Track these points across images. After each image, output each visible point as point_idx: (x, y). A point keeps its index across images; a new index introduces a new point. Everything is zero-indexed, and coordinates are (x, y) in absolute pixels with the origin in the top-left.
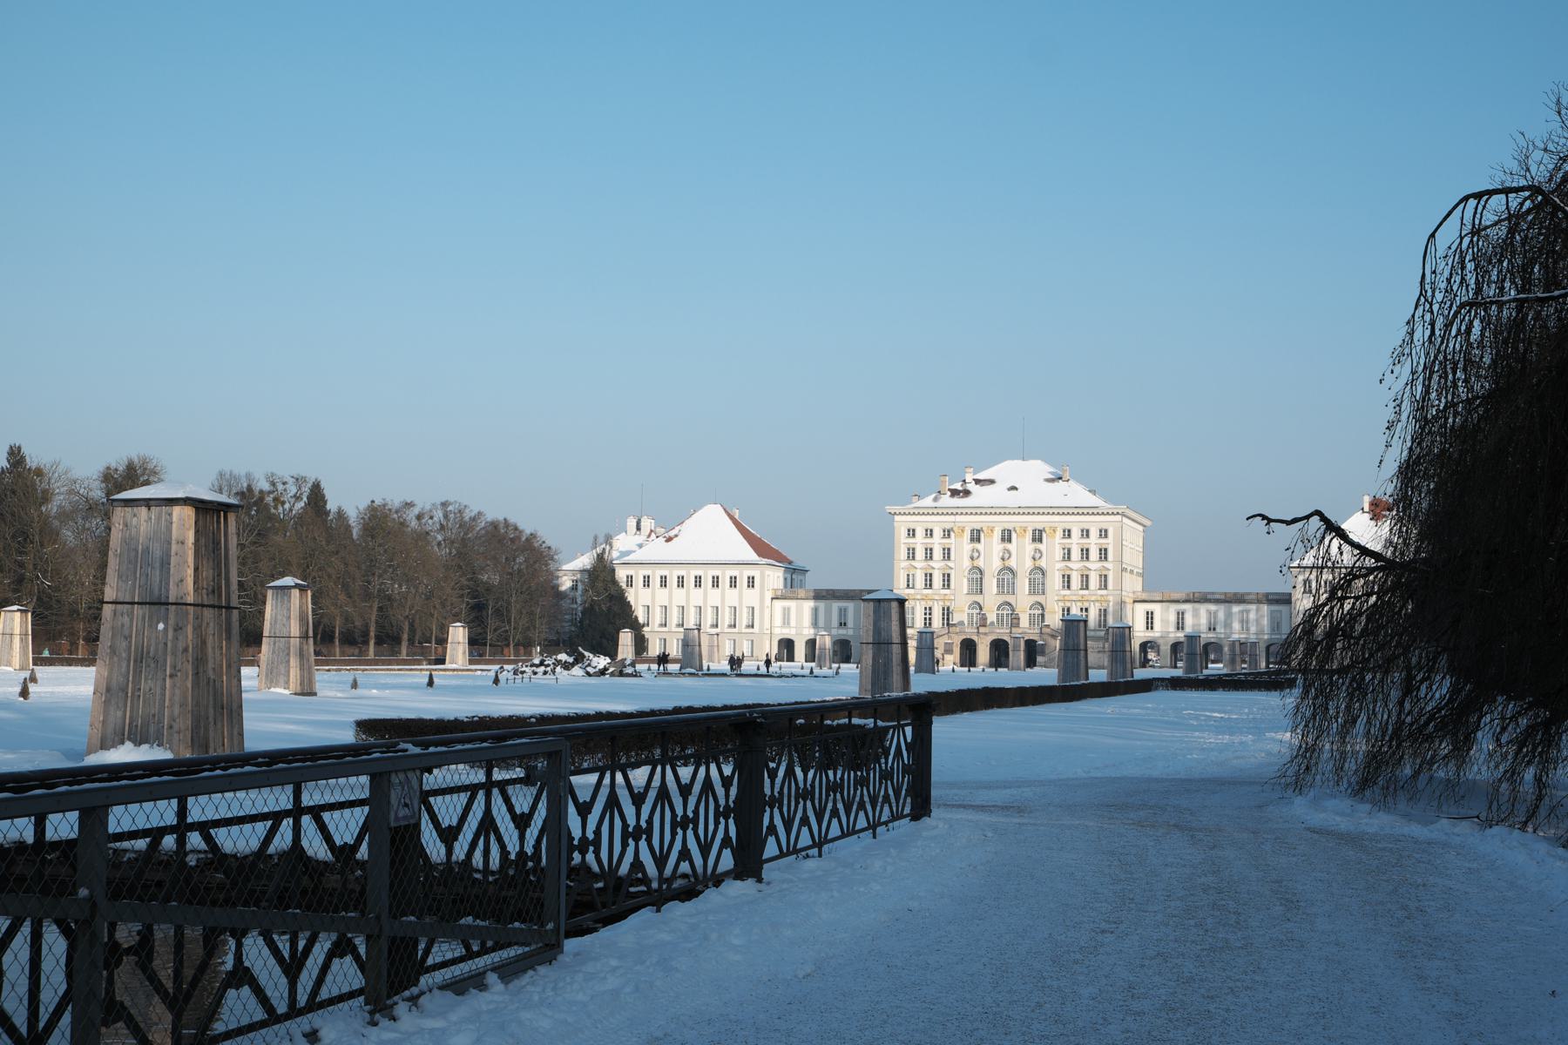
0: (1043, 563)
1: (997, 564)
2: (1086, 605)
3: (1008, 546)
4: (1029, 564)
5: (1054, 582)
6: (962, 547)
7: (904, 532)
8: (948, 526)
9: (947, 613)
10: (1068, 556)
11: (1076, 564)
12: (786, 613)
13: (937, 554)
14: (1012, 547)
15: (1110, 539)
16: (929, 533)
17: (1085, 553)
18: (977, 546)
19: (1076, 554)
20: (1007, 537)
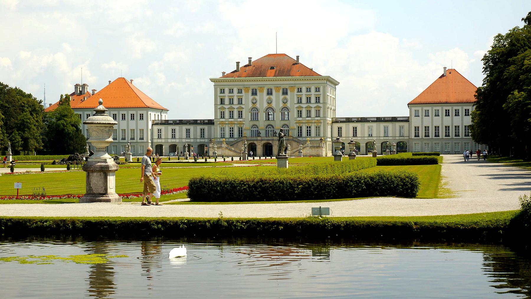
0: (288, 105)
1: (266, 105)
3: (271, 96)
4: (281, 105)
6: (247, 98)
7: (219, 91)
10: (300, 101)
12: (159, 131)
13: (236, 101)
14: (273, 97)
19: (304, 100)
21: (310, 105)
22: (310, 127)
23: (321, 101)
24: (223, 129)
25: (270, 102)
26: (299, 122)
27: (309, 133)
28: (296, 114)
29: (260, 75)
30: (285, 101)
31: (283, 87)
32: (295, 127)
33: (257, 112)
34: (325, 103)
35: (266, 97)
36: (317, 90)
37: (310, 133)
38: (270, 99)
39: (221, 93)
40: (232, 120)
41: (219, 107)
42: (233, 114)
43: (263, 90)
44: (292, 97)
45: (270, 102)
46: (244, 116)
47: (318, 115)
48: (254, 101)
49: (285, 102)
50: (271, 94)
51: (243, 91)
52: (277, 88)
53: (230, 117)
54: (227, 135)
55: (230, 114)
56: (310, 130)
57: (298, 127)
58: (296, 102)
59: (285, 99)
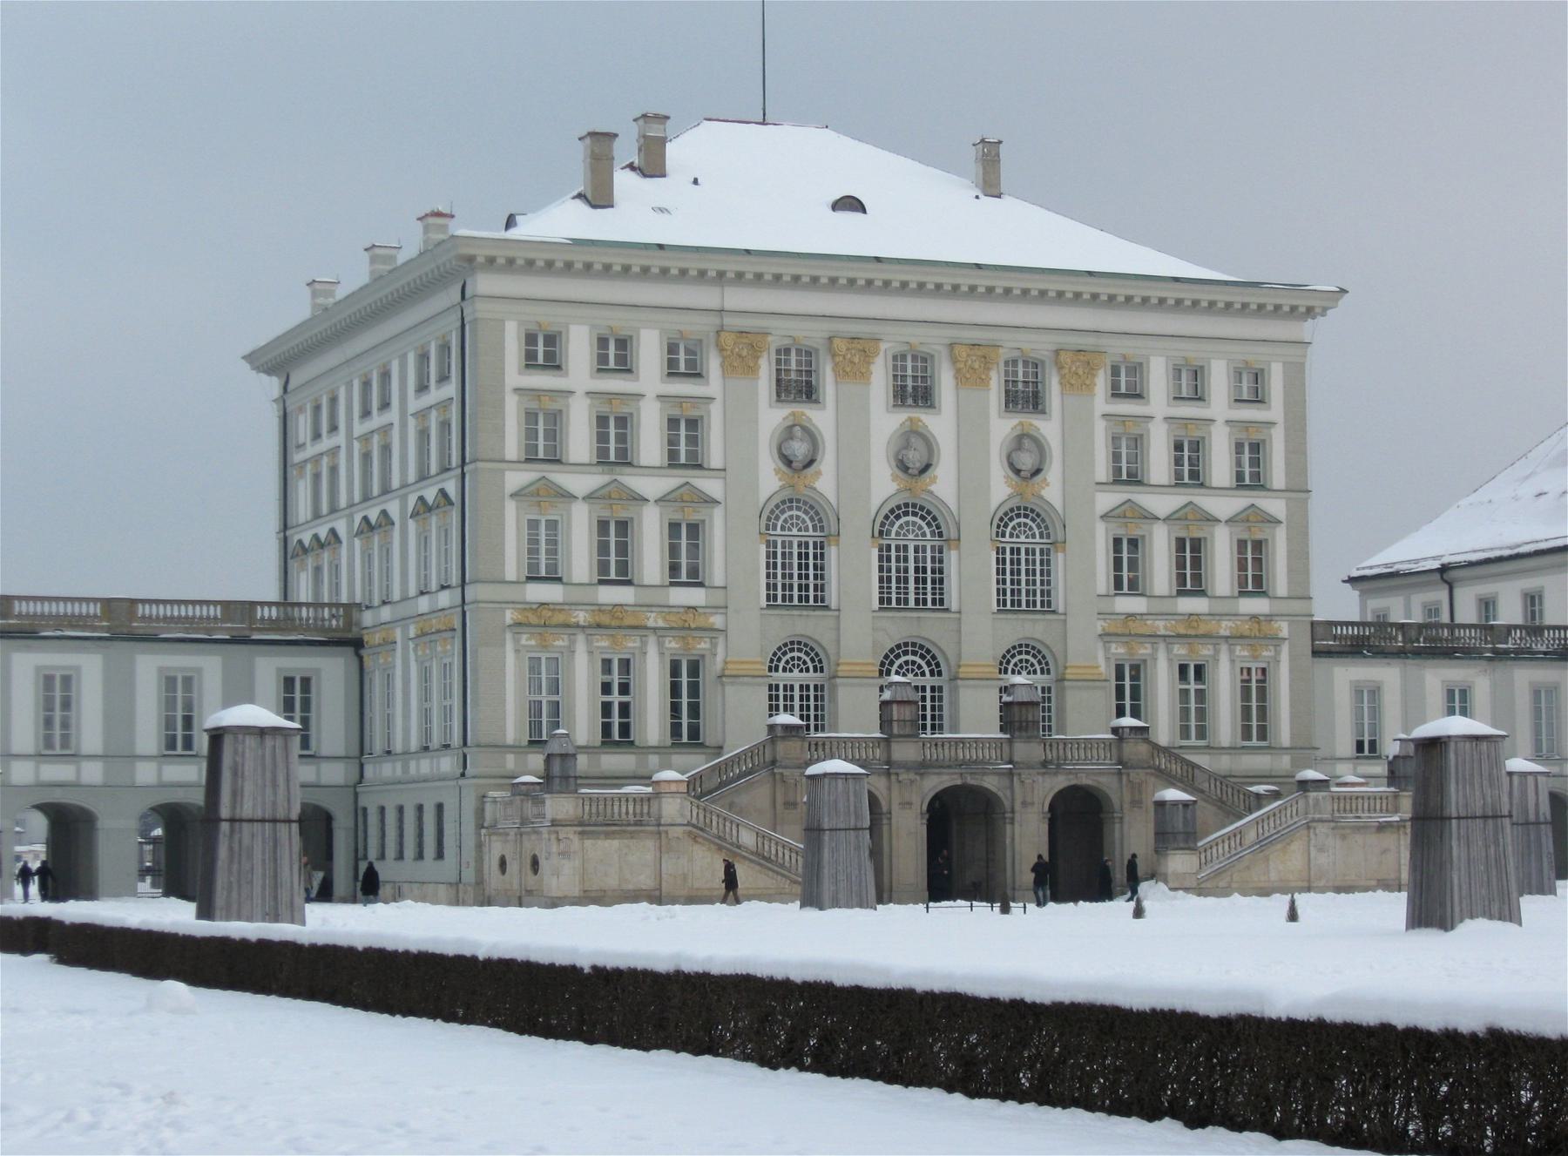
0: (1052, 489)
1: (884, 486)
2: (1206, 651)
4: (1000, 489)
9: (687, 683)
14: (940, 424)
15: (1275, 410)
16: (616, 354)
22: (1199, 670)
23: (1277, 475)
25: (914, 461)
26: (1124, 630)
28: (1102, 578)
30: (1026, 461)
31: (1011, 344)
32: (1105, 670)
34: (1298, 490)
35: (885, 422)
37: (1201, 714)
38: (913, 436)
39: (530, 362)
40: (623, 595)
43: (867, 356)
45: (914, 461)
47: (1253, 580)
49: (1026, 463)
51: (713, 365)
52: (974, 358)
53: (603, 567)
54: (583, 725)
56: (1201, 695)
57: (1119, 671)
58: (1102, 471)
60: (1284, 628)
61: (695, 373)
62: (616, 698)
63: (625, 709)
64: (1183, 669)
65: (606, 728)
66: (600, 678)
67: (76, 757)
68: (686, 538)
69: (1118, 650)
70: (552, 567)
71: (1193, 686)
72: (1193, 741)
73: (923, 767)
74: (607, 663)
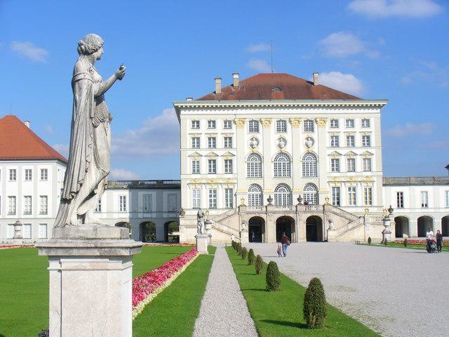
0: (315, 149)
1: (274, 151)
2: (354, 185)
3: (284, 135)
4: (303, 150)
5: (325, 165)
6: (242, 136)
7: (189, 124)
8: (229, 118)
11: (344, 151)
13: (220, 142)
14: (287, 136)
16: (212, 124)
17: (351, 138)
18: (255, 135)
19: (343, 141)
20: (282, 126)
21: (355, 151)
22: (354, 190)
24: (197, 193)
27: (354, 201)
29: (260, 98)
31: (305, 117)
33: (259, 162)
36: (366, 122)
41: (190, 153)
42: (215, 166)
44: (322, 135)
46: (235, 171)
48: (255, 142)
50: (285, 130)
51: (233, 126)
53: (210, 170)
54: (205, 204)
55: (210, 166)
56: (355, 195)
59: (312, 139)
60: (375, 179)
61: (230, 127)
62: (213, 198)
63: (215, 201)
64: (350, 189)
65: (211, 205)
66: (209, 194)
67: (151, 212)
68: (229, 163)
69: (333, 185)
70: (198, 171)
71: (352, 192)
72: (352, 205)
73: (274, 213)
74: (211, 191)
